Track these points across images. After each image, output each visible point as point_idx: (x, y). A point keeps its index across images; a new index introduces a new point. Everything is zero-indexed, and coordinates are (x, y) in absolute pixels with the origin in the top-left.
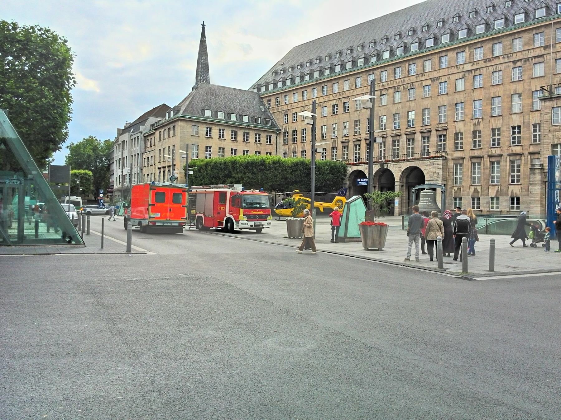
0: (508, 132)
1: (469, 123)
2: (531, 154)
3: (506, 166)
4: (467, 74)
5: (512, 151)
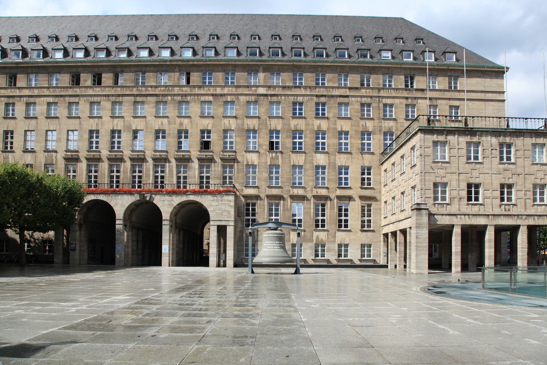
0: (312, 171)
1: (264, 156)
2: (339, 198)
3: (310, 208)
4: (262, 98)
5: (317, 192)
